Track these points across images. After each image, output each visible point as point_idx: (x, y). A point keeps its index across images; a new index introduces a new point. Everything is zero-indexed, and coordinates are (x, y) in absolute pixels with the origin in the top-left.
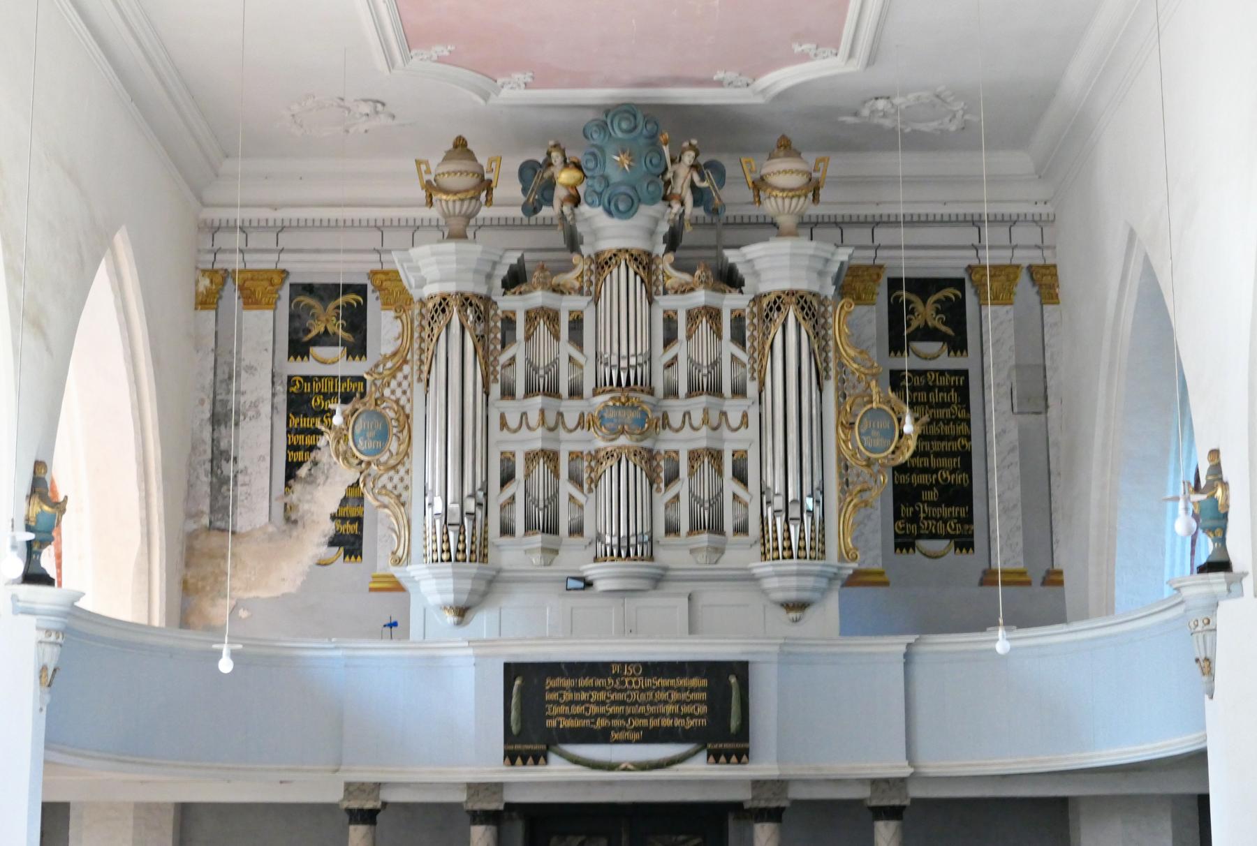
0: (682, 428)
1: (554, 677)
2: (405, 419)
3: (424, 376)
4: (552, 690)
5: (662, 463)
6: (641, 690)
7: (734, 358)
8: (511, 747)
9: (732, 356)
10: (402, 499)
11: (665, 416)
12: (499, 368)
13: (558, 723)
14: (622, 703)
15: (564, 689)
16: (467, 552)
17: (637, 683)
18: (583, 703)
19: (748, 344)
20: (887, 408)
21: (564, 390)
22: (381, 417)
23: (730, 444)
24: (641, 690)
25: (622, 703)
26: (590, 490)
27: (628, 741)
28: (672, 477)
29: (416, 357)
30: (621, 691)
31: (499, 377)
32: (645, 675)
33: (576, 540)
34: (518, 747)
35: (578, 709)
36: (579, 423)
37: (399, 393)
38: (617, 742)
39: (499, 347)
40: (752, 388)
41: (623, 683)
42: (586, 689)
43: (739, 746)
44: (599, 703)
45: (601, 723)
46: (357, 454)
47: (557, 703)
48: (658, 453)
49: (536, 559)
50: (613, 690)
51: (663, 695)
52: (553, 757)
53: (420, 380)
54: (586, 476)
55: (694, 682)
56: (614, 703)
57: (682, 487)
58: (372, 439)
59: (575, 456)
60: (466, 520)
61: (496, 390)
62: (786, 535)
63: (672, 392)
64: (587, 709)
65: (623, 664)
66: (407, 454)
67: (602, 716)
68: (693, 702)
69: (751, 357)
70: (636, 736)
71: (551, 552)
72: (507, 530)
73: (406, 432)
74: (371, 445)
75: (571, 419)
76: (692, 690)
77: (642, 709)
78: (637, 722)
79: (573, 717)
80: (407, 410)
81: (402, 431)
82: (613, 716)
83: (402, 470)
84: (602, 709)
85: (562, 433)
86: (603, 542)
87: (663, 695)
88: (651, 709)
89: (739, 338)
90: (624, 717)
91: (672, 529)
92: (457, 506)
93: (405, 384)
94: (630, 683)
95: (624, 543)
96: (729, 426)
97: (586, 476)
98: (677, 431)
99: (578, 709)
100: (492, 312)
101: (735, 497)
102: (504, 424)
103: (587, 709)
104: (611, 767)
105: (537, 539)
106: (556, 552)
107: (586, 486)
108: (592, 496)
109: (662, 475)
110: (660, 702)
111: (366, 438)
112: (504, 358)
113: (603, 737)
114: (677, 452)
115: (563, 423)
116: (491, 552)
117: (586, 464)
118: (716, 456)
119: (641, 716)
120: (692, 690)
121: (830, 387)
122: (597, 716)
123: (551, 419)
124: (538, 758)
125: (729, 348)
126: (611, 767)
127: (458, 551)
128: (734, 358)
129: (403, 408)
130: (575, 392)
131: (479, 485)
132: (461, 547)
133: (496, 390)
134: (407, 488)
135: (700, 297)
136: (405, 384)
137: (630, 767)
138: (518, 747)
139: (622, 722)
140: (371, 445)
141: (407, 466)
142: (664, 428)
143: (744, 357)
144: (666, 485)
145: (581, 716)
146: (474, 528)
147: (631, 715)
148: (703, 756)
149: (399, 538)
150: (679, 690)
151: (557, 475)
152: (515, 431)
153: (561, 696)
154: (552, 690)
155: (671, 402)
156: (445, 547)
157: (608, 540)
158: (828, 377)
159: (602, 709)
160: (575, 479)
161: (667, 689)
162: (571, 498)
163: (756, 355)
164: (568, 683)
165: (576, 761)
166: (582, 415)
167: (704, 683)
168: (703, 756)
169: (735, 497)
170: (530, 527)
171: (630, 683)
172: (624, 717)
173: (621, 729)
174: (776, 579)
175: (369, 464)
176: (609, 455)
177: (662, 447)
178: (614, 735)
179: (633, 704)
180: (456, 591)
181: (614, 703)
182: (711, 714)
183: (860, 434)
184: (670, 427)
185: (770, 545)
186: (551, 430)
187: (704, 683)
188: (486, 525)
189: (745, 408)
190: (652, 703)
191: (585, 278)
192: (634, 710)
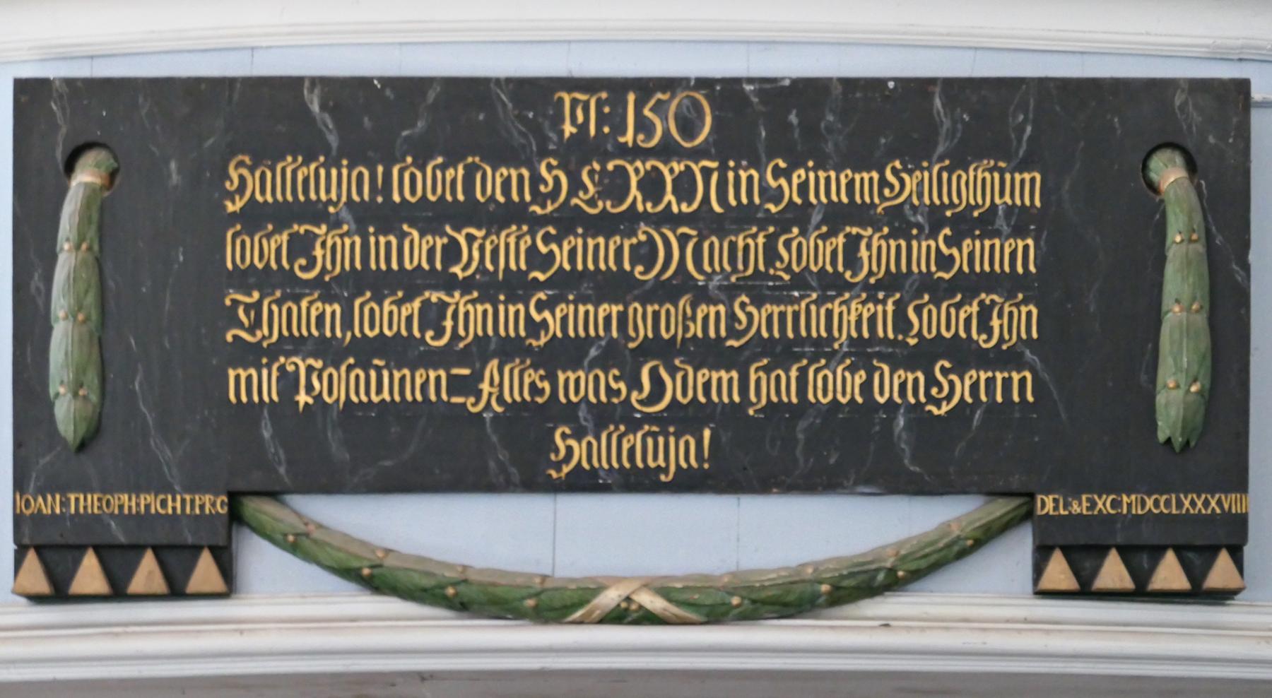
1: (265, 155)
4: (254, 217)
6: (706, 222)
8: (49, 505)
13: (288, 382)
14: (611, 286)
15: (316, 213)
17: (684, 187)
18: (408, 283)
24: (706, 222)
25: (611, 286)
27: (639, 481)
30: (604, 225)
32: (732, 145)
34: (86, 502)
35: (392, 316)
38: (585, 482)
41: (615, 186)
42: (431, 216)
43: (1194, 504)
44: (488, 287)
45: (504, 384)
47: (292, 288)
50: (568, 221)
51: (816, 251)
52: (260, 559)
55: (977, 185)
56: (569, 284)
64: (433, 317)
65: (616, 88)
67: (509, 349)
68: (969, 285)
70: (681, 452)
76: (968, 224)
77: (709, 319)
78: (686, 384)
79: (365, 352)
82: (566, 353)
84: (511, 318)
87: (816, 251)
88: (761, 319)
90: (619, 356)
94: (652, 185)
99: (392, 316)
103: (433, 317)
104: (553, 604)
110: (800, 281)
113: (513, 457)
119: (708, 353)
120: (968, 224)
122: (481, 351)
124: (188, 560)
126: (553, 604)
138: (86, 502)
139: (611, 379)
145: (400, 351)
147: (659, 348)
148: (1017, 550)
150: (898, 222)
153: (302, 246)
154: (254, 217)
159: (511, 318)
161: (837, 216)
164: (339, 184)
165: (375, 576)
167: (1026, 188)
168: (1017, 550)
171: (652, 185)
172: (619, 356)
173: (606, 415)
178: (576, 451)
179: (665, 291)
181: (569, 284)
182: (1055, 346)
187: (1026, 188)
190: (760, 289)
192: (675, 319)
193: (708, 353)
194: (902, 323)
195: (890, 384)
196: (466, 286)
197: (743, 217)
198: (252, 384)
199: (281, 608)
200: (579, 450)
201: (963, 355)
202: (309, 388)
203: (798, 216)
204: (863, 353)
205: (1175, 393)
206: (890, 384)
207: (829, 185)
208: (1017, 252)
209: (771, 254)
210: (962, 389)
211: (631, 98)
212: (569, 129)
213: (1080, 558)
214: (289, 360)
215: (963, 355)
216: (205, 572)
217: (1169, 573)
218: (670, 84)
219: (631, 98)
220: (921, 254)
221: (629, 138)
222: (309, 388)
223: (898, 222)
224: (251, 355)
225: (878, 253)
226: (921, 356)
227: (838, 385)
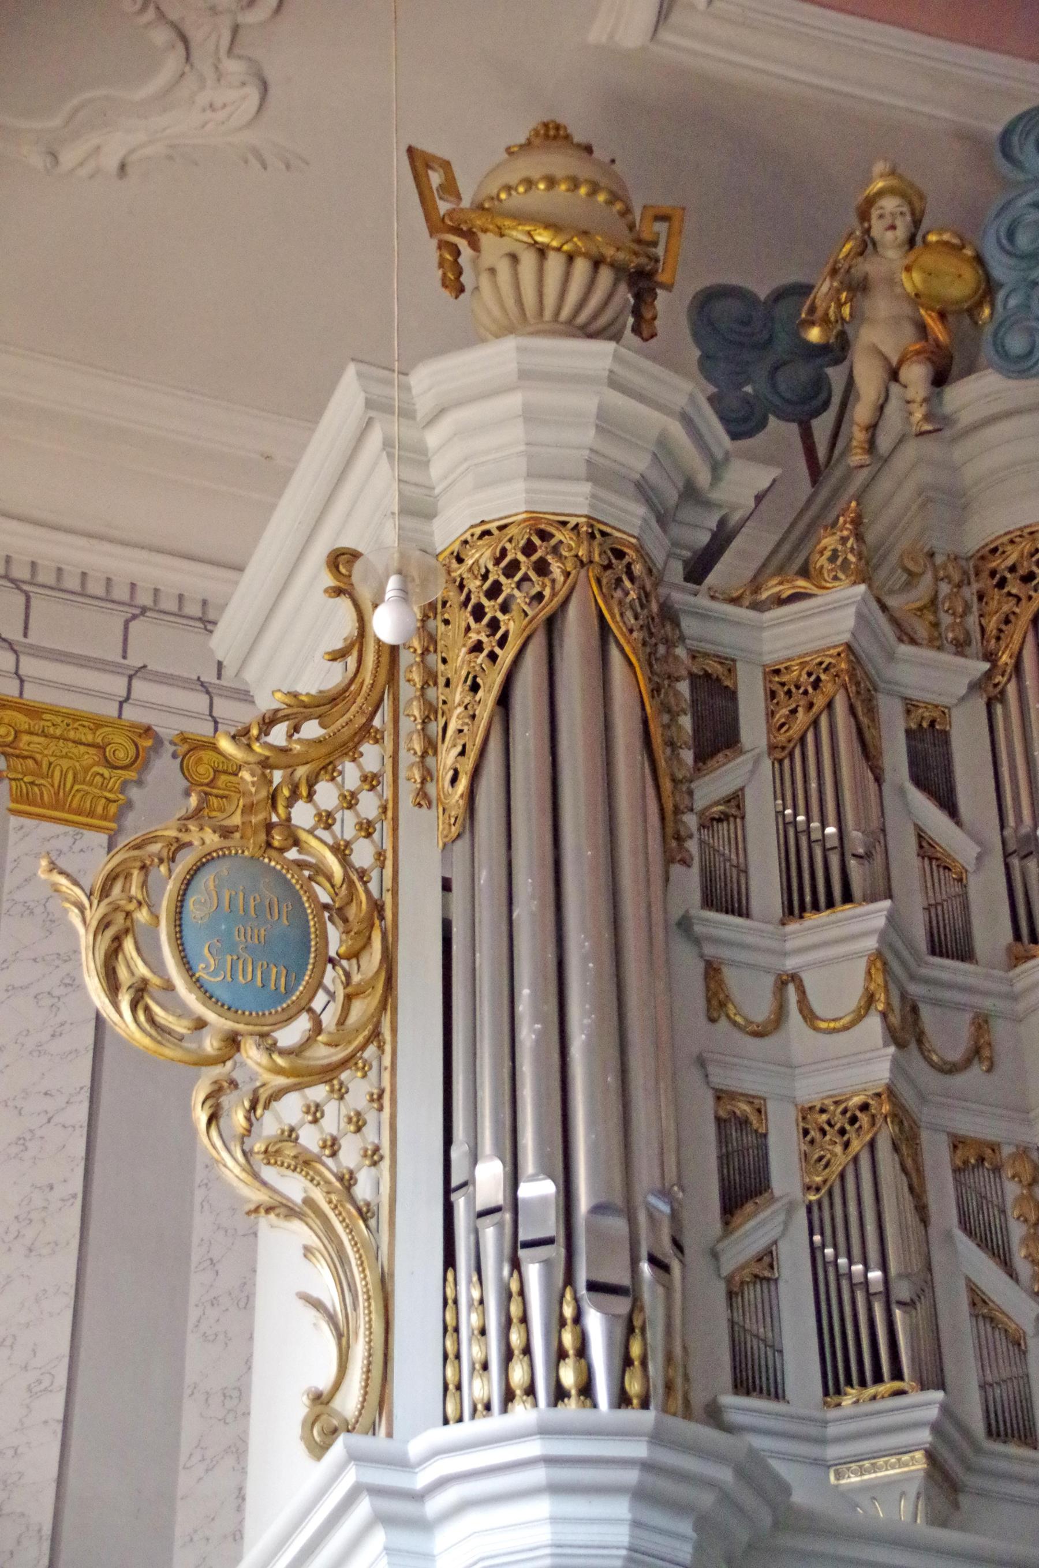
12: (691, 820)
31: (692, 846)
39: (688, 756)
66: (376, 1035)
81: (355, 955)
93: (369, 805)
112: (711, 789)
136: (369, 805)
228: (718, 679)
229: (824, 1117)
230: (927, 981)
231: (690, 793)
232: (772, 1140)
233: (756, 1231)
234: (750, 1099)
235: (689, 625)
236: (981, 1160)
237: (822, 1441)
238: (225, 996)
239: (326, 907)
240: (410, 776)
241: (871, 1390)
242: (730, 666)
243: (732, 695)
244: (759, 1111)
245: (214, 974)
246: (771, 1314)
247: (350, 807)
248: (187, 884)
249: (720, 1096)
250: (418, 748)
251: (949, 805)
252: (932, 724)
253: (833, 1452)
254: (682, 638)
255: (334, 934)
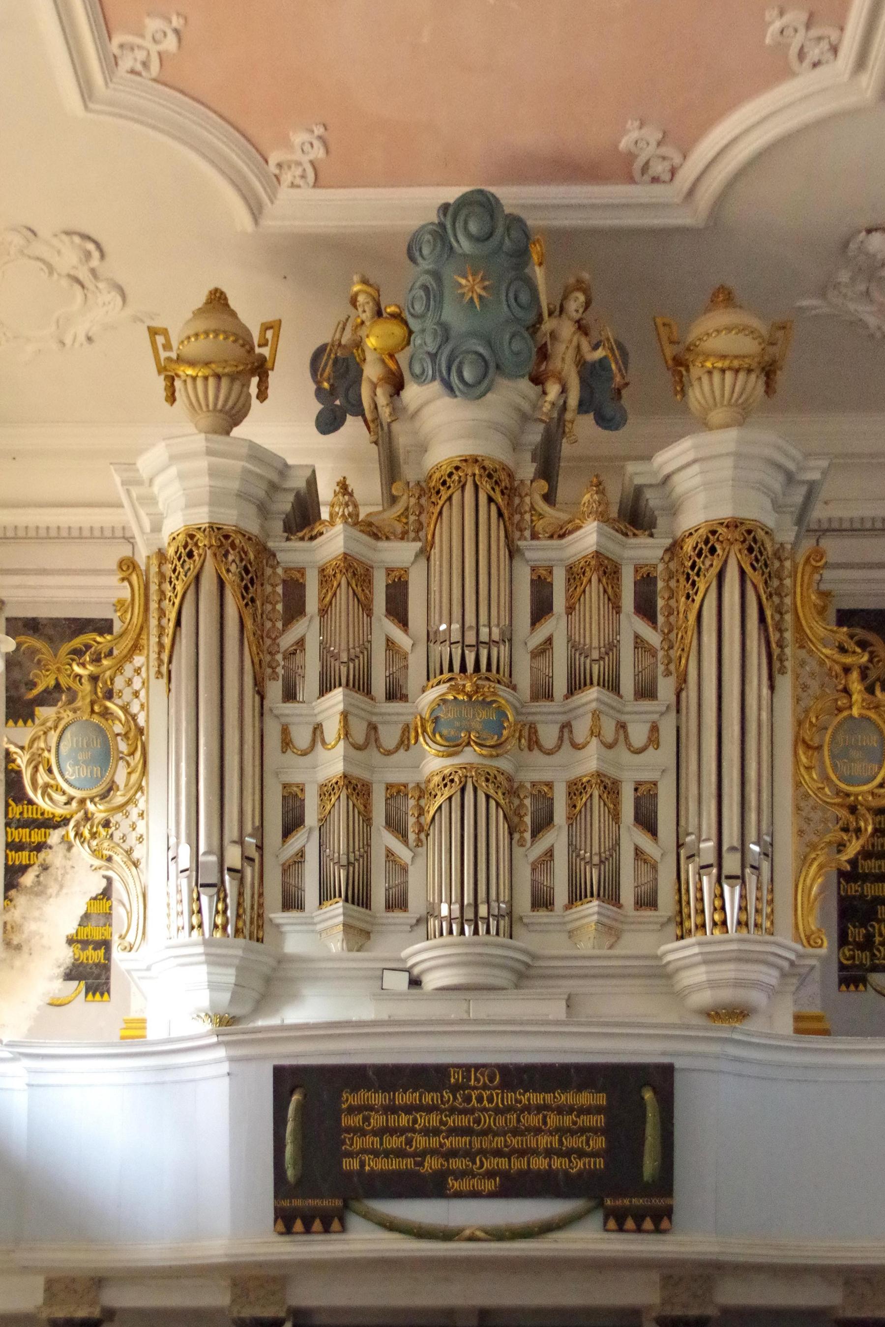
0: (559, 747)
2: (137, 734)
3: (164, 669)
5: (527, 802)
7: (639, 642)
9: (637, 636)
10: (135, 855)
11: (533, 730)
12: (279, 657)
16: (230, 929)
19: (661, 619)
20: (872, 714)
21: (379, 686)
22: (101, 731)
23: (631, 771)
26: (419, 843)
27: (475, 1195)
28: (543, 823)
29: (154, 640)
31: (280, 671)
33: (398, 915)
36: (402, 742)
37: (127, 695)
39: (279, 625)
40: (666, 688)
45: (432, 1164)
46: (65, 786)
48: (522, 786)
49: (336, 944)
53: (159, 673)
54: (412, 820)
57: (557, 838)
58: (87, 763)
59: (396, 792)
60: (227, 878)
61: (274, 690)
62: (717, 903)
63: (543, 692)
64: (409, 1142)
66: (140, 788)
67: (433, 1152)
69: (666, 637)
71: (359, 935)
72: (292, 901)
73: (138, 754)
74: (85, 772)
75: (389, 736)
79: (387, 1154)
80: (141, 721)
81: (132, 754)
83: (134, 812)
85: (375, 757)
86: (438, 916)
89: (646, 608)
91: (542, 900)
92: (213, 859)
95: (469, 914)
96: (629, 746)
97: (412, 820)
98: (549, 753)
100: (269, 571)
101: (638, 852)
102: (287, 743)
103: (409, 1142)
104: (448, 1235)
105: (336, 909)
106: (367, 934)
107: (412, 837)
108: (421, 850)
109: (528, 819)
111: (76, 763)
112: (287, 641)
113: (434, 1187)
114: (550, 785)
115: (377, 740)
116: (268, 934)
117: (412, 802)
118: (610, 788)
121: (785, 683)
122: (423, 1154)
123: (359, 732)
125: (632, 624)
126: (448, 1235)
127: (216, 926)
128: (639, 642)
129: (134, 717)
130: (395, 693)
131: (249, 828)
132: (219, 920)
133: (274, 690)
134: (140, 839)
135: (588, 538)
137: (479, 1234)
140: (85, 772)
141: (142, 805)
142: (530, 749)
143: (653, 637)
144: (534, 835)
145: (400, 1153)
146: (241, 894)
149: (129, 914)
151: (368, 821)
152: (304, 754)
155: (544, 706)
156: (195, 921)
157: (444, 910)
158: (783, 671)
160: (396, 826)
162: (389, 854)
163: (672, 636)
165: (391, 1226)
166: (406, 729)
169: (638, 852)
170: (325, 896)
174: (703, 969)
175: (82, 801)
176: (447, 780)
177: (528, 777)
178: (454, 1184)
180: (213, 986)
183: (833, 757)
184: (541, 748)
185: (692, 923)
186: (358, 748)
188: (261, 895)
189: (655, 717)
191: (412, 518)
193: (498, 1153)
194: (561, 1142)
195: (558, 1163)
196: (420, 1132)
197: (509, 1109)
198: (350, 1164)
199: (361, 1239)
200: (456, 1185)
201: (581, 1154)
202: (369, 1165)
203: (527, 1108)
204: (549, 1153)
205: (649, 1166)
206: (558, 1163)
207: (536, 1098)
208: (599, 1120)
209: (519, 1121)
210: (580, 1164)
211: (473, 1070)
212: (452, 1080)
213: (618, 1220)
214: (362, 1157)
215: (581, 1154)
216: (336, 1225)
217: (648, 1224)
218: (484, 1066)
219: (473, 1070)
220: (567, 1121)
221: (472, 1083)
222: (369, 1165)
223: (560, 1110)
224: (350, 1155)
225: (553, 1120)
226: (567, 1154)
227: (540, 1163)
228: (297, 580)
229: (326, 789)
230: (381, 714)
231: (278, 645)
232: (307, 802)
233: (297, 841)
234: (298, 785)
235: (280, 556)
236: (399, 792)
237: (315, 924)
238: (77, 785)
239: (118, 735)
240: (153, 663)
241: (330, 902)
242: (302, 571)
243: (303, 586)
244: (302, 790)
245: (72, 775)
246: (300, 876)
247: (129, 685)
248: (60, 738)
249: (285, 786)
250: (156, 650)
251: (403, 621)
252: (400, 579)
253: (319, 927)
254: (278, 563)
255: (123, 746)
